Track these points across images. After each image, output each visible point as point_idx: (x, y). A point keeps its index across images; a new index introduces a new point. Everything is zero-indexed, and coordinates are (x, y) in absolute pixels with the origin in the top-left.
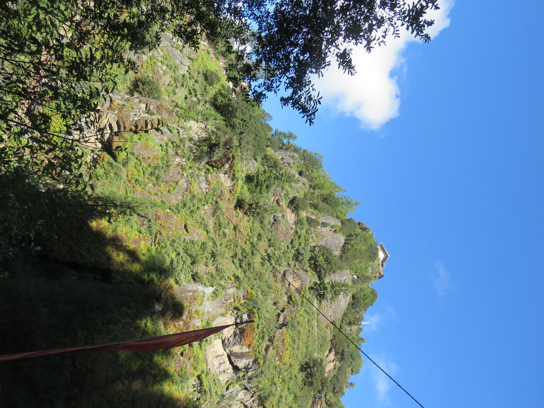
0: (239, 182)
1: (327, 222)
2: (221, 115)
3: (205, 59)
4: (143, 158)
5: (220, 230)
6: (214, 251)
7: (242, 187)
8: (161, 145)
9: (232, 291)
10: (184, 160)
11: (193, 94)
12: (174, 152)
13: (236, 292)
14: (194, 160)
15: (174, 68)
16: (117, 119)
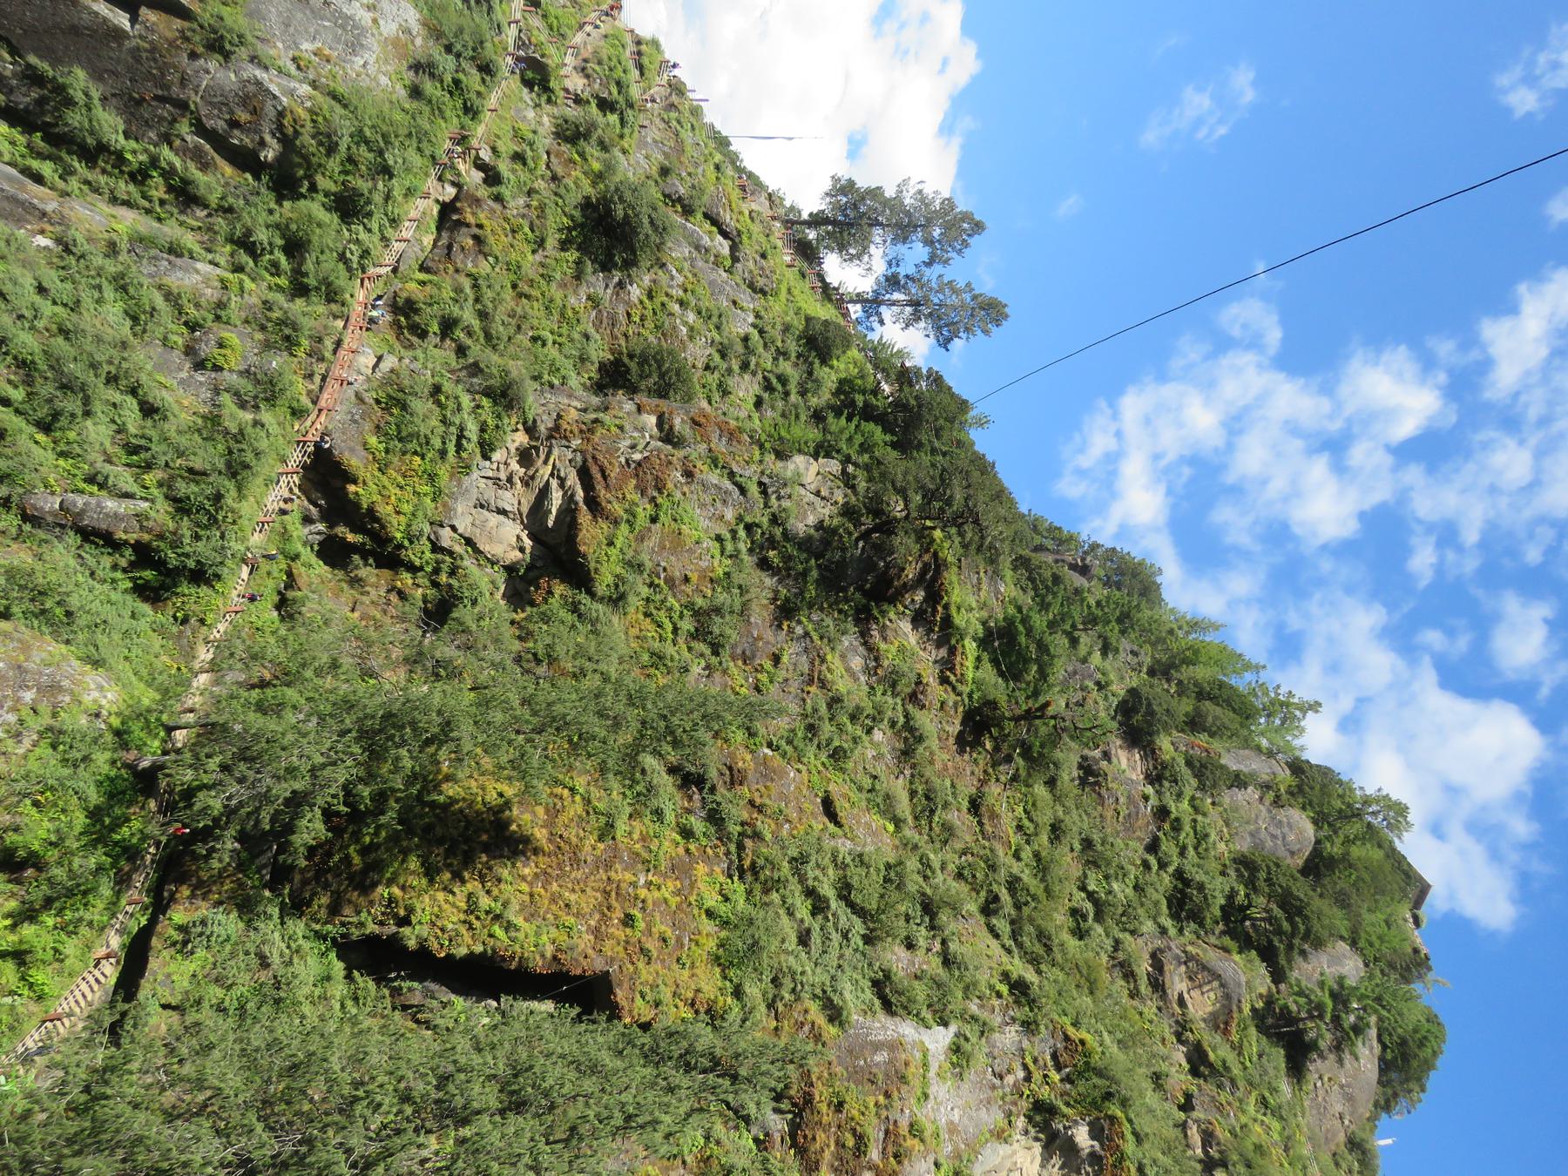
1: (1245, 770)
2: (885, 431)
3: (796, 292)
4: (670, 581)
5: (932, 812)
6: (929, 891)
7: (978, 659)
8: (719, 538)
9: (1010, 1037)
13: (1026, 1044)
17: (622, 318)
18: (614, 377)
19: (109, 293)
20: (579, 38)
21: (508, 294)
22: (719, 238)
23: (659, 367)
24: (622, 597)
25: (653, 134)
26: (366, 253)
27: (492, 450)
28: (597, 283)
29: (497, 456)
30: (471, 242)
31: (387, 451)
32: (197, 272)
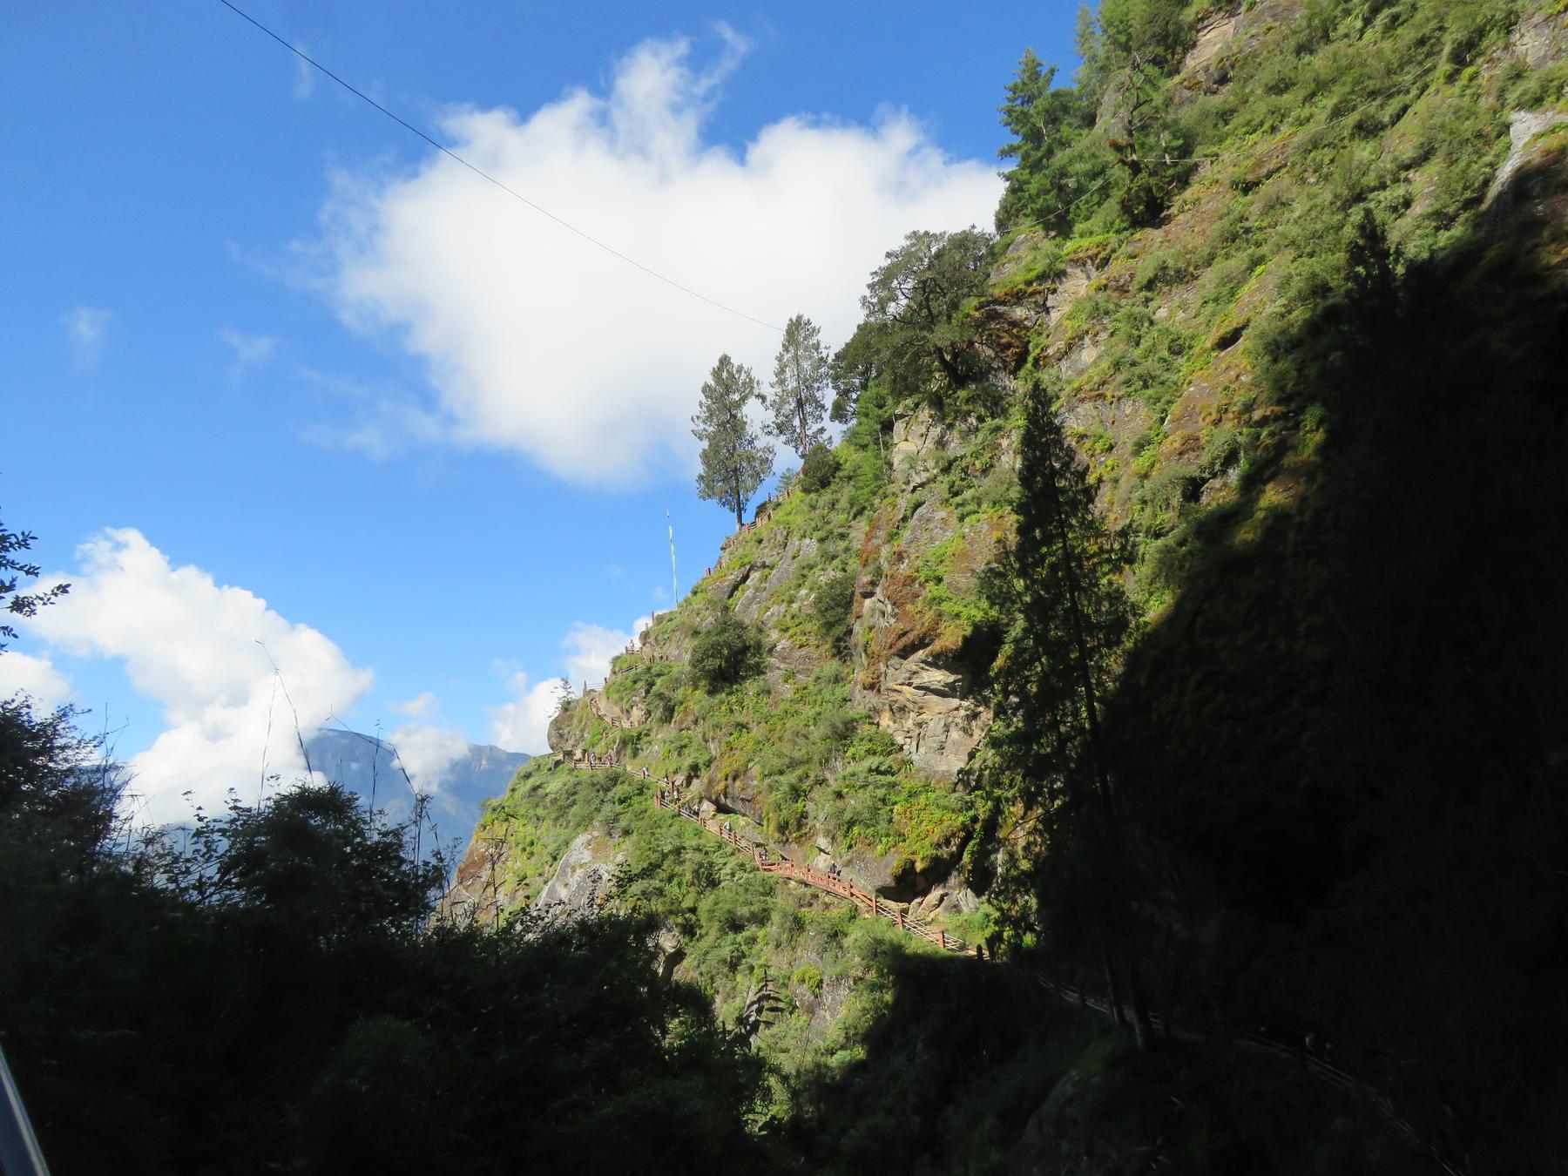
5: (1247, 231)
7: (1082, 236)
8: (962, 519)
10: (1005, 443)
13: (1537, 19)
16: (895, 661)
17: (803, 652)
25: (671, 650)
26: (742, 866)
29: (900, 740)
30: (738, 783)
31: (888, 835)
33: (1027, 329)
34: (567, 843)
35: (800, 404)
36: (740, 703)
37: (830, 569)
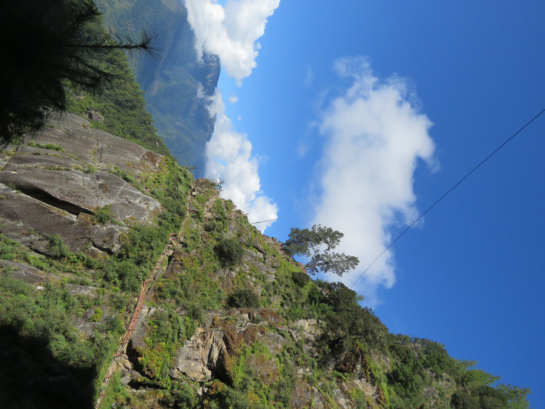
0: (382, 384)
2: (329, 305)
3: (287, 266)
4: (262, 377)
7: (389, 390)
8: (278, 356)
10: (308, 370)
11: (289, 298)
12: (293, 363)
14: (320, 367)
15: (262, 278)
16: (222, 335)
17: (231, 283)
18: (232, 302)
19: (60, 301)
20: (207, 203)
21: (192, 280)
22: (259, 253)
23: (246, 297)
24: (245, 387)
26: (145, 275)
27: (190, 336)
28: (222, 273)
29: (192, 338)
30: (179, 266)
32: (89, 289)
33: (352, 372)
34: (158, 198)
35: (327, 263)
36: (211, 261)
37: (263, 289)
